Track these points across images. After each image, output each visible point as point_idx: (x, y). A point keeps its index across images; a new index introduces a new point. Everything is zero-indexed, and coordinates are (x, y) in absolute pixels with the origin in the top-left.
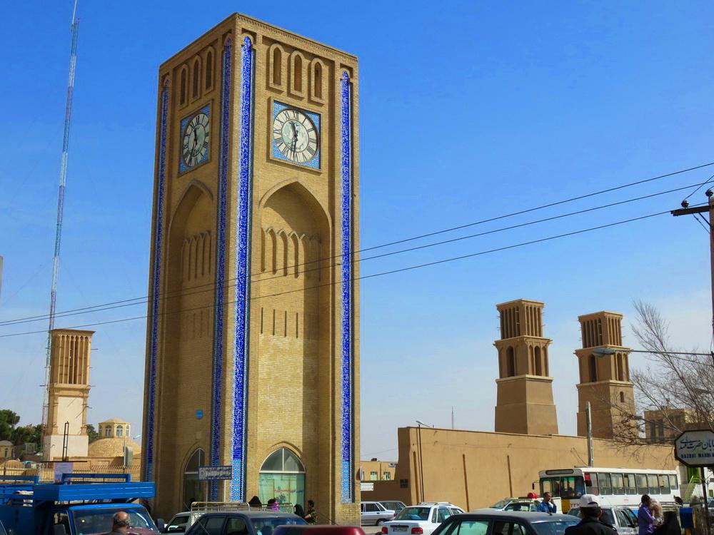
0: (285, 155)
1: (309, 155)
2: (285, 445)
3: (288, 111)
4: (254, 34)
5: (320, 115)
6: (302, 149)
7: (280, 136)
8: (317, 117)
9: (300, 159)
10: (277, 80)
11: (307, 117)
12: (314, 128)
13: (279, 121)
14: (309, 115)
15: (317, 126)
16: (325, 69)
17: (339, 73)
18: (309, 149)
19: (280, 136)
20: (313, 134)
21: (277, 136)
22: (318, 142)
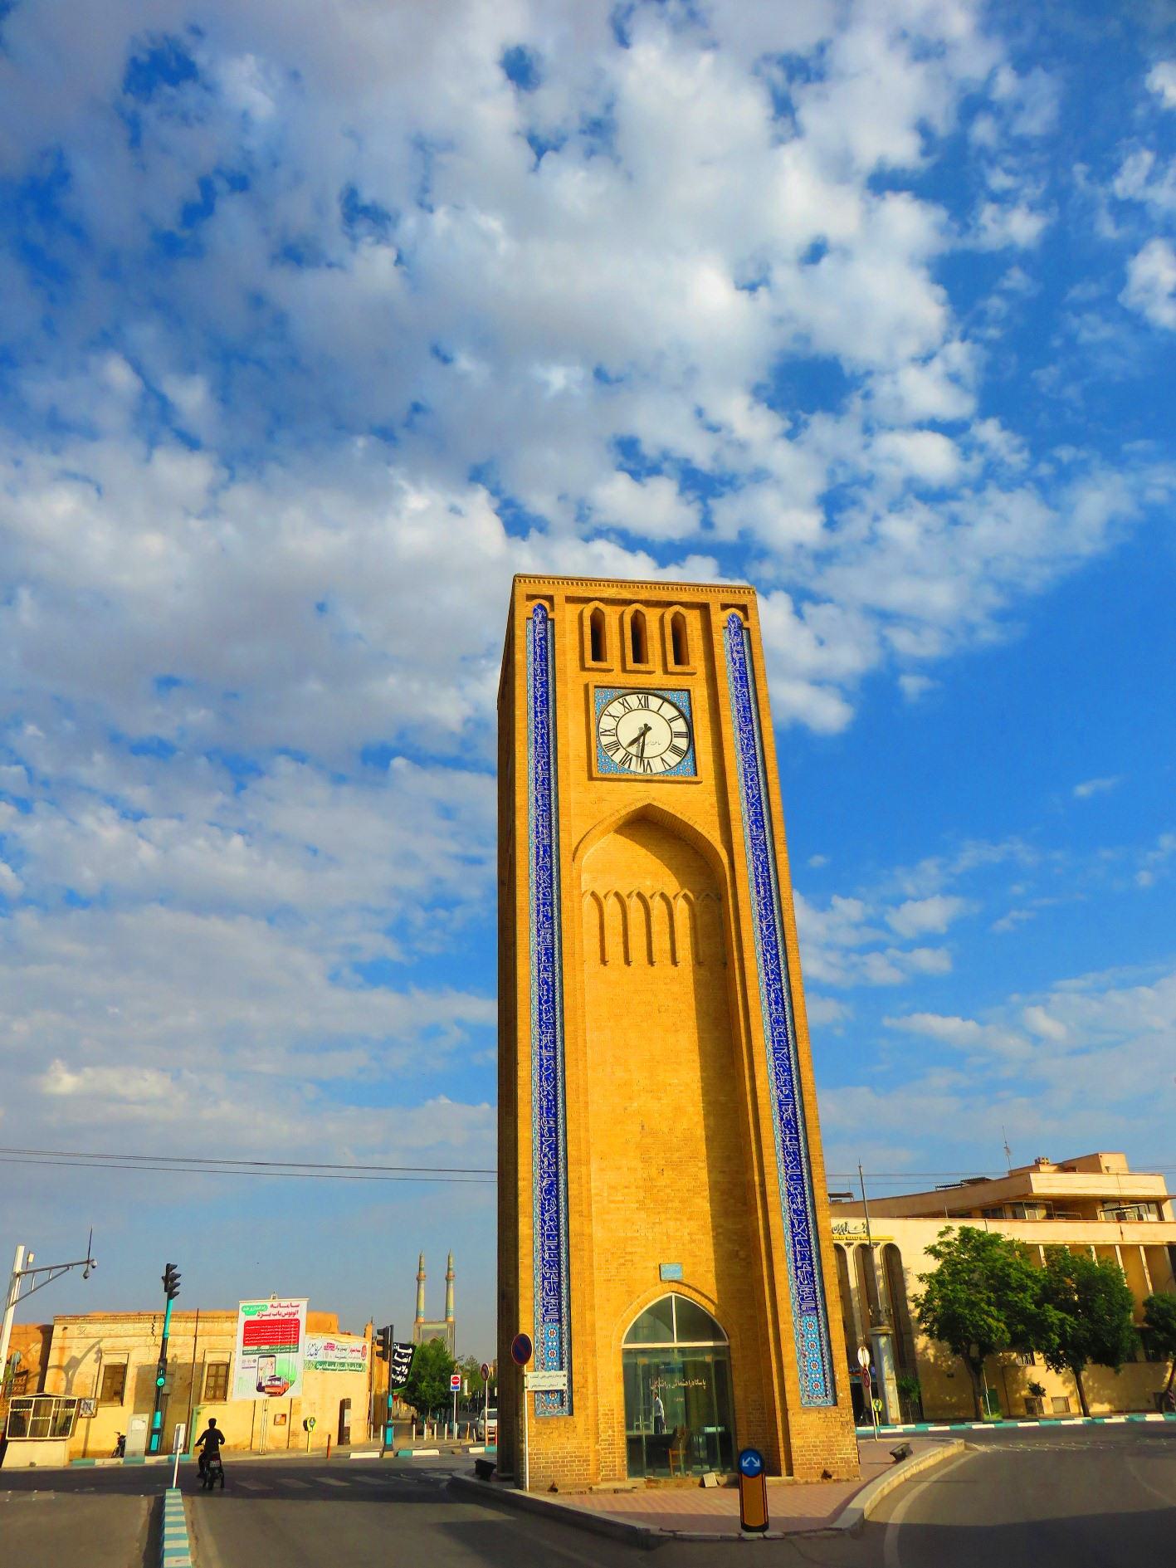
1: (673, 759)
2: (686, 1290)
3: (627, 698)
5: (689, 691)
7: (614, 738)
9: (658, 767)
10: (598, 654)
11: (665, 700)
12: (682, 715)
14: (667, 695)
15: (686, 711)
16: (693, 620)
17: (719, 618)
18: (674, 749)
19: (614, 738)
20: (680, 725)
21: (605, 740)
22: (690, 735)
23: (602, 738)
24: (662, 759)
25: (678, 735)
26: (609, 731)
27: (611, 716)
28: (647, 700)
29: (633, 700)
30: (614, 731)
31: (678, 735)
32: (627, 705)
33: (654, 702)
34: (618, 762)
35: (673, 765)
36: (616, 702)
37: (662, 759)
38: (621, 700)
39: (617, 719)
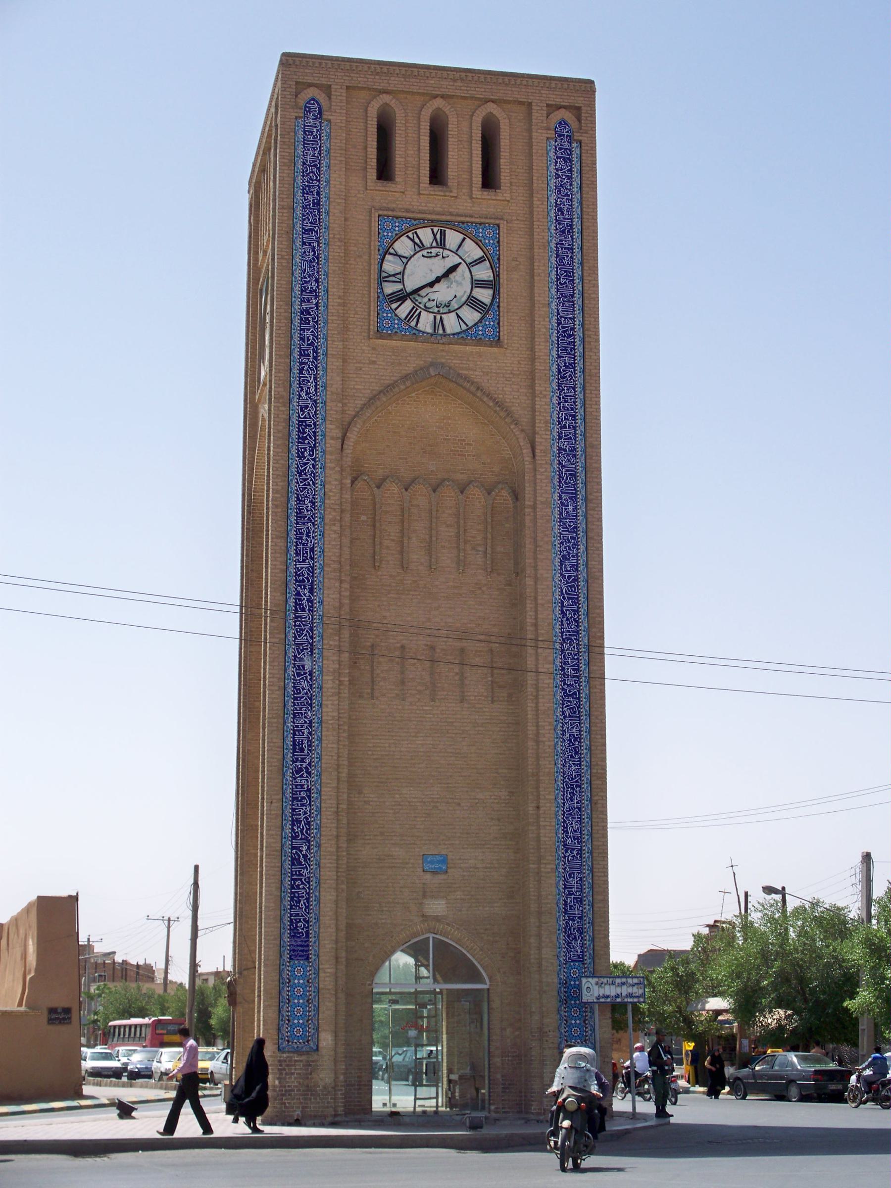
0: (413, 324)
1: (471, 316)
3: (419, 231)
4: (327, 90)
6: (454, 305)
8: (489, 232)
10: (385, 171)
13: (396, 255)
23: (385, 284)
24: (458, 316)
25: (478, 284)
26: (394, 275)
27: (400, 256)
28: (443, 234)
29: (426, 235)
30: (400, 276)
31: (478, 284)
32: (417, 240)
33: (453, 238)
34: (403, 316)
35: (470, 324)
36: (404, 238)
37: (458, 316)
38: (410, 234)
39: (405, 260)
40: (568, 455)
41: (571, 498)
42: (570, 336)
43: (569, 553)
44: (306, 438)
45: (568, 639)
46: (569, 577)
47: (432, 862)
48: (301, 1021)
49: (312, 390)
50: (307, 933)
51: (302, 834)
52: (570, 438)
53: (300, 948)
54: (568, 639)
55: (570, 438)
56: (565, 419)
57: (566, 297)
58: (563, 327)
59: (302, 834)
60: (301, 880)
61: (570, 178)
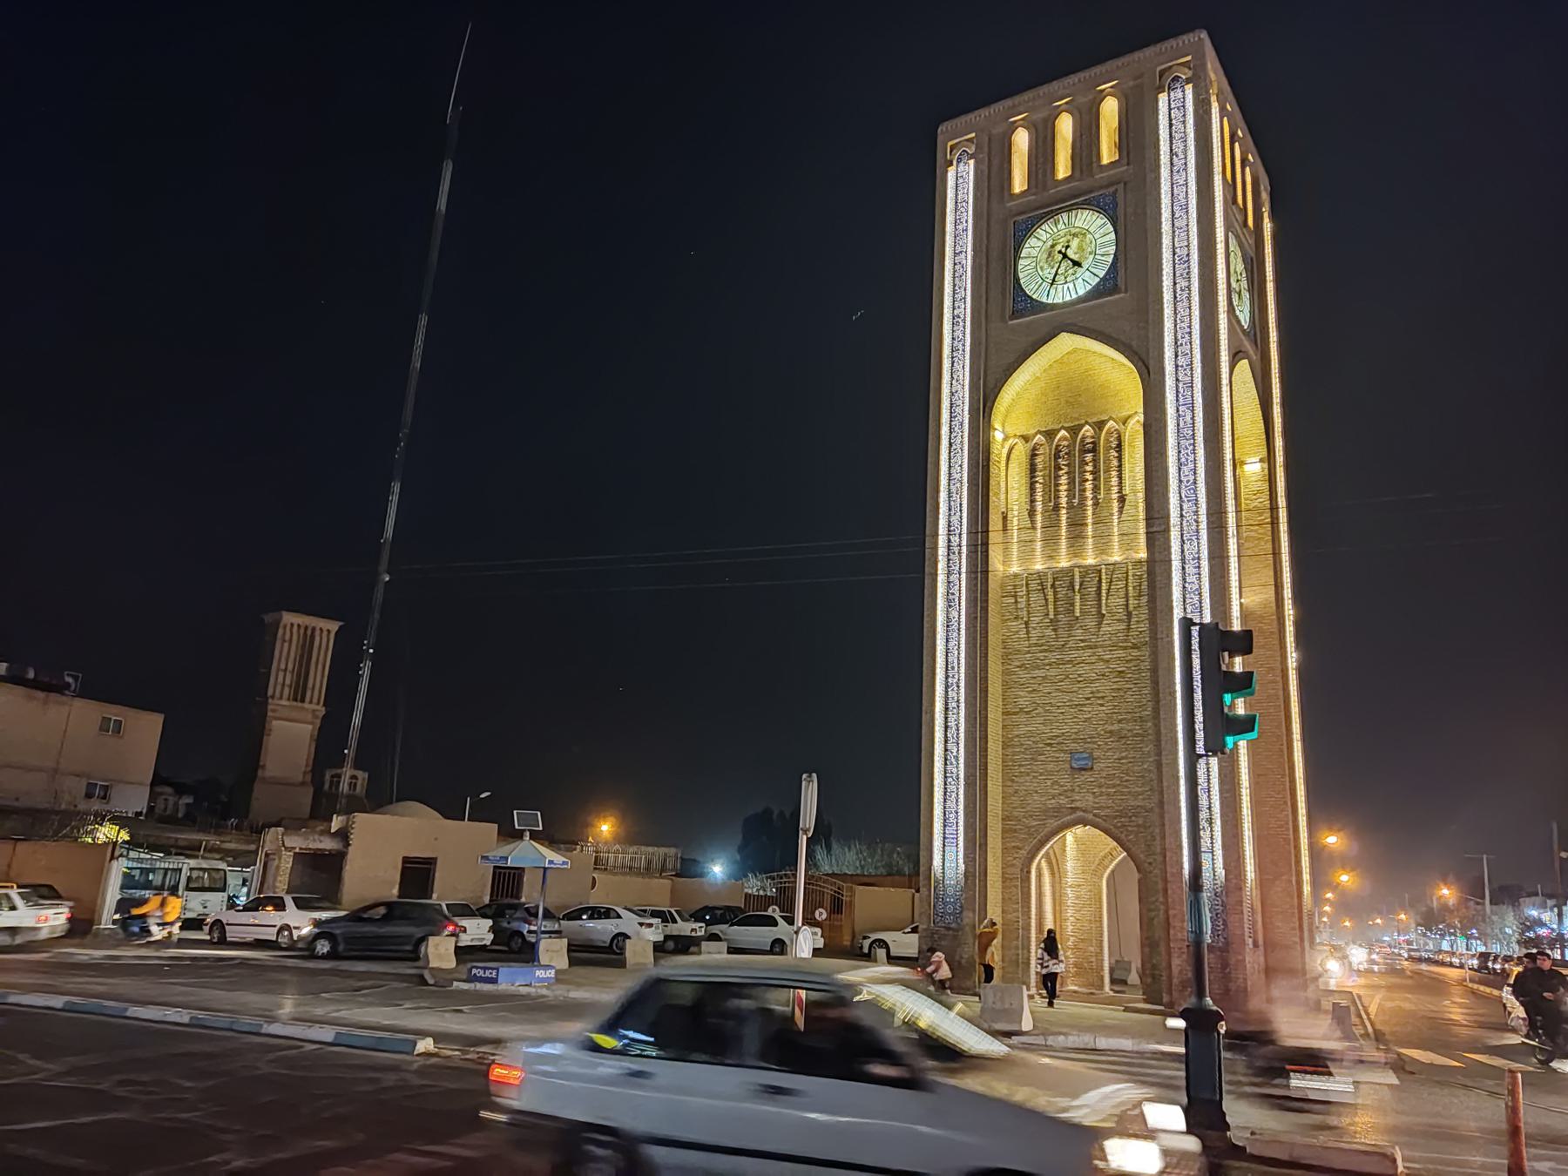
40: (1185, 370)
41: (1188, 409)
42: (1185, 262)
43: (1187, 460)
44: (956, 416)
45: (1188, 540)
46: (1188, 481)
47: (1079, 759)
48: (952, 900)
49: (961, 376)
50: (957, 823)
51: (953, 738)
52: (1187, 354)
53: (952, 836)
54: (1188, 540)
55: (1187, 354)
56: (1182, 338)
57: (1181, 228)
58: (1179, 256)
59: (953, 738)
60: (952, 777)
61: (1184, 122)
